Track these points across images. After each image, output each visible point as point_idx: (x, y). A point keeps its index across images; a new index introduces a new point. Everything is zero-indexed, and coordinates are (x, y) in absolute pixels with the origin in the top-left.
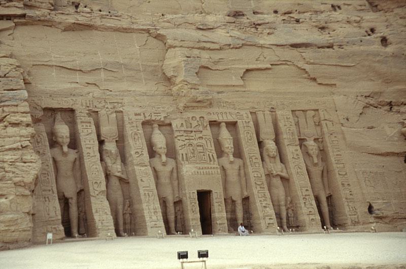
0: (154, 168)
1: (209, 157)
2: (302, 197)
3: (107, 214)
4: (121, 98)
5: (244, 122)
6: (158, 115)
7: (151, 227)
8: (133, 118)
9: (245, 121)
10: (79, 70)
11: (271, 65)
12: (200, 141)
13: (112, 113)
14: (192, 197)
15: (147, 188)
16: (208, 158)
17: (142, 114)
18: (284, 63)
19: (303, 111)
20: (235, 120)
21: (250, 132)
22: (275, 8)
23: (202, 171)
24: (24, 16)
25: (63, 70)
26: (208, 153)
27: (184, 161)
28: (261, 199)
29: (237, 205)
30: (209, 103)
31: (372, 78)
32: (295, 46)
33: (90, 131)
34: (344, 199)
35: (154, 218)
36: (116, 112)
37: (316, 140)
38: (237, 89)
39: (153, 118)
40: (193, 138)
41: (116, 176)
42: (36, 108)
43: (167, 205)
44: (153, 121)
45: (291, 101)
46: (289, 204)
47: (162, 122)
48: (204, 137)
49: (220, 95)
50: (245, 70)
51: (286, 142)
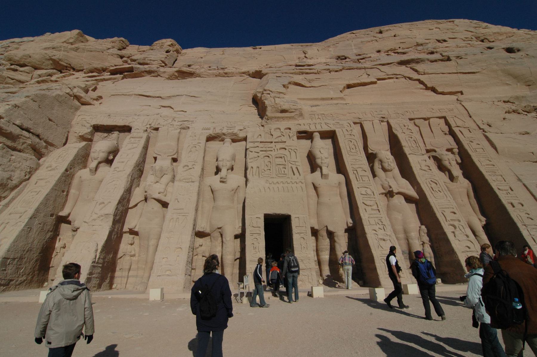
12: (283, 151)
15: (179, 211)
17: (212, 129)
19: (425, 119)
21: (353, 141)
22: (377, 50)
24: (131, 70)
26: (290, 165)
28: (376, 227)
29: (336, 239)
30: (297, 112)
31: (507, 82)
32: (402, 63)
34: (519, 225)
36: (184, 129)
39: (225, 131)
44: (224, 134)
45: (407, 110)
47: (235, 135)
50: (345, 85)
51: (407, 150)
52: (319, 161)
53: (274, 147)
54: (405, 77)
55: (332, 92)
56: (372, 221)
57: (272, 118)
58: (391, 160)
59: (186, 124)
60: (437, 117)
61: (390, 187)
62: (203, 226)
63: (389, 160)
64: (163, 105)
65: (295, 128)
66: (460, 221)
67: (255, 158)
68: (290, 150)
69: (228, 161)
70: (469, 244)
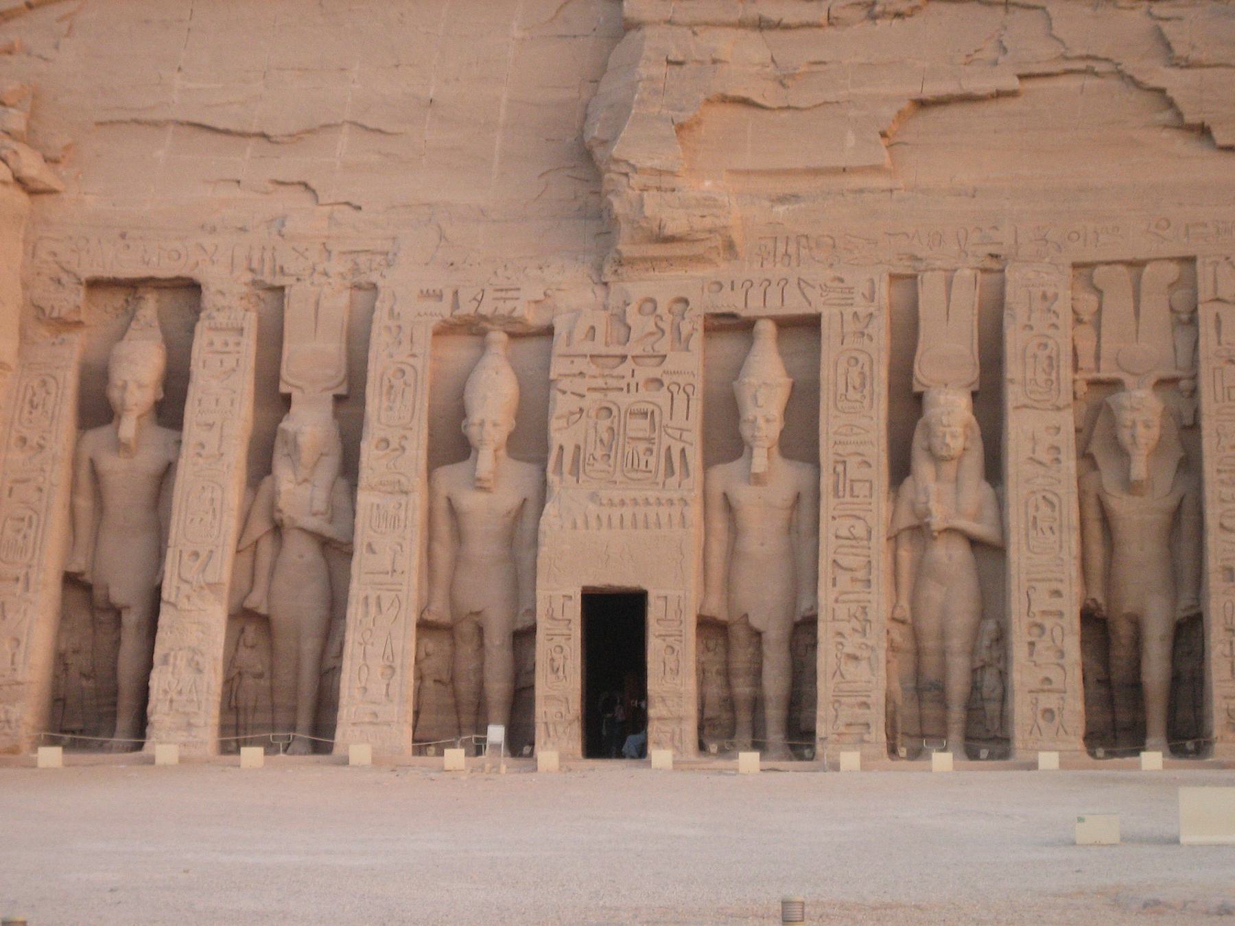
0: (449, 500)
1: (669, 458)
2: (1026, 621)
3: (200, 671)
5: (848, 317)
6: (510, 294)
7: (354, 724)
9: (855, 313)
10: (255, 135)
11: (1021, 77)
14: (558, 614)
16: (663, 460)
17: (448, 296)
18: (1081, 65)
19: (1130, 264)
20: (811, 311)
21: (863, 358)
23: (616, 513)
25: (207, 136)
27: (561, 474)
28: (846, 627)
30: (718, 241)
33: (230, 362)
35: (377, 688)
37: (1162, 383)
38: (856, 181)
39: (486, 309)
40: (623, 384)
41: (303, 530)
42: (59, 281)
43: (486, 641)
44: (484, 318)
46: (990, 647)
47: (520, 321)
49: (780, 209)
50: (905, 105)
51: (1013, 395)
52: (746, 432)
53: (628, 379)
54: (1121, 74)
55: (851, 140)
56: (842, 611)
57: (632, 262)
58: (959, 430)
60: (1171, 259)
61: (928, 513)
63: (947, 430)
64: (281, 179)
65: (704, 302)
66: (1060, 614)
67: (573, 414)
68: (674, 388)
69: (495, 425)
70: (1055, 675)
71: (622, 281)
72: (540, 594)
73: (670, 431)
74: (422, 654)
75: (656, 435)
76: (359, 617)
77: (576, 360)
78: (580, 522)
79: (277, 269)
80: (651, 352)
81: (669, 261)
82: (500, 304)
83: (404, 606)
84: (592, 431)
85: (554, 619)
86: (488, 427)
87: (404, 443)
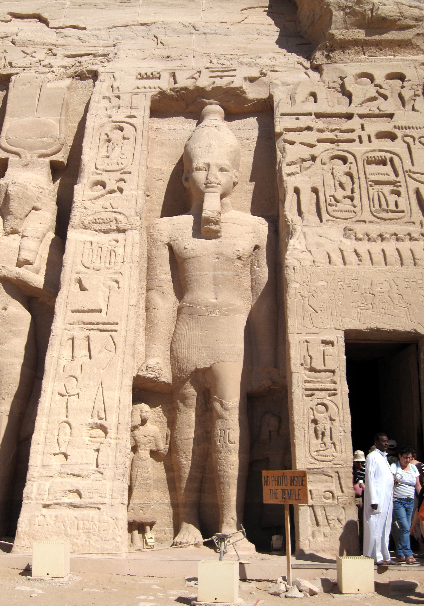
4: (111, 43)
7: (46, 506)
8: (127, 83)
13: (61, 79)
14: (318, 364)
17: (166, 77)
23: (376, 248)
35: (82, 456)
36: (80, 77)
39: (205, 82)
48: (399, 133)
59: (88, 64)
62: (152, 362)
67: (303, 160)
68: (410, 140)
69: (222, 170)
71: (335, 62)
72: (295, 338)
73: (414, 175)
74: (138, 421)
75: (401, 178)
76: (63, 362)
77: (300, 117)
78: (336, 258)
79: (7, 64)
80: (377, 112)
81: (380, 46)
82: (217, 80)
83: (120, 351)
84: (328, 176)
85: (312, 370)
86: (214, 170)
87: (121, 184)
